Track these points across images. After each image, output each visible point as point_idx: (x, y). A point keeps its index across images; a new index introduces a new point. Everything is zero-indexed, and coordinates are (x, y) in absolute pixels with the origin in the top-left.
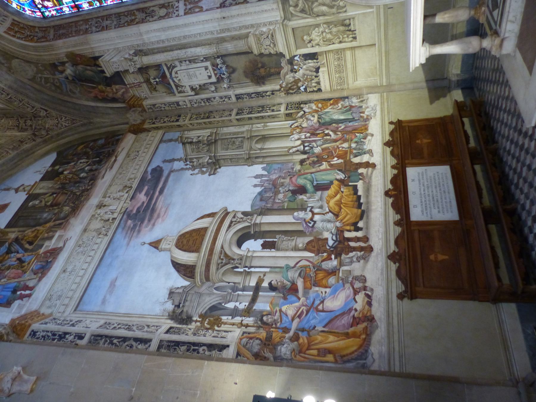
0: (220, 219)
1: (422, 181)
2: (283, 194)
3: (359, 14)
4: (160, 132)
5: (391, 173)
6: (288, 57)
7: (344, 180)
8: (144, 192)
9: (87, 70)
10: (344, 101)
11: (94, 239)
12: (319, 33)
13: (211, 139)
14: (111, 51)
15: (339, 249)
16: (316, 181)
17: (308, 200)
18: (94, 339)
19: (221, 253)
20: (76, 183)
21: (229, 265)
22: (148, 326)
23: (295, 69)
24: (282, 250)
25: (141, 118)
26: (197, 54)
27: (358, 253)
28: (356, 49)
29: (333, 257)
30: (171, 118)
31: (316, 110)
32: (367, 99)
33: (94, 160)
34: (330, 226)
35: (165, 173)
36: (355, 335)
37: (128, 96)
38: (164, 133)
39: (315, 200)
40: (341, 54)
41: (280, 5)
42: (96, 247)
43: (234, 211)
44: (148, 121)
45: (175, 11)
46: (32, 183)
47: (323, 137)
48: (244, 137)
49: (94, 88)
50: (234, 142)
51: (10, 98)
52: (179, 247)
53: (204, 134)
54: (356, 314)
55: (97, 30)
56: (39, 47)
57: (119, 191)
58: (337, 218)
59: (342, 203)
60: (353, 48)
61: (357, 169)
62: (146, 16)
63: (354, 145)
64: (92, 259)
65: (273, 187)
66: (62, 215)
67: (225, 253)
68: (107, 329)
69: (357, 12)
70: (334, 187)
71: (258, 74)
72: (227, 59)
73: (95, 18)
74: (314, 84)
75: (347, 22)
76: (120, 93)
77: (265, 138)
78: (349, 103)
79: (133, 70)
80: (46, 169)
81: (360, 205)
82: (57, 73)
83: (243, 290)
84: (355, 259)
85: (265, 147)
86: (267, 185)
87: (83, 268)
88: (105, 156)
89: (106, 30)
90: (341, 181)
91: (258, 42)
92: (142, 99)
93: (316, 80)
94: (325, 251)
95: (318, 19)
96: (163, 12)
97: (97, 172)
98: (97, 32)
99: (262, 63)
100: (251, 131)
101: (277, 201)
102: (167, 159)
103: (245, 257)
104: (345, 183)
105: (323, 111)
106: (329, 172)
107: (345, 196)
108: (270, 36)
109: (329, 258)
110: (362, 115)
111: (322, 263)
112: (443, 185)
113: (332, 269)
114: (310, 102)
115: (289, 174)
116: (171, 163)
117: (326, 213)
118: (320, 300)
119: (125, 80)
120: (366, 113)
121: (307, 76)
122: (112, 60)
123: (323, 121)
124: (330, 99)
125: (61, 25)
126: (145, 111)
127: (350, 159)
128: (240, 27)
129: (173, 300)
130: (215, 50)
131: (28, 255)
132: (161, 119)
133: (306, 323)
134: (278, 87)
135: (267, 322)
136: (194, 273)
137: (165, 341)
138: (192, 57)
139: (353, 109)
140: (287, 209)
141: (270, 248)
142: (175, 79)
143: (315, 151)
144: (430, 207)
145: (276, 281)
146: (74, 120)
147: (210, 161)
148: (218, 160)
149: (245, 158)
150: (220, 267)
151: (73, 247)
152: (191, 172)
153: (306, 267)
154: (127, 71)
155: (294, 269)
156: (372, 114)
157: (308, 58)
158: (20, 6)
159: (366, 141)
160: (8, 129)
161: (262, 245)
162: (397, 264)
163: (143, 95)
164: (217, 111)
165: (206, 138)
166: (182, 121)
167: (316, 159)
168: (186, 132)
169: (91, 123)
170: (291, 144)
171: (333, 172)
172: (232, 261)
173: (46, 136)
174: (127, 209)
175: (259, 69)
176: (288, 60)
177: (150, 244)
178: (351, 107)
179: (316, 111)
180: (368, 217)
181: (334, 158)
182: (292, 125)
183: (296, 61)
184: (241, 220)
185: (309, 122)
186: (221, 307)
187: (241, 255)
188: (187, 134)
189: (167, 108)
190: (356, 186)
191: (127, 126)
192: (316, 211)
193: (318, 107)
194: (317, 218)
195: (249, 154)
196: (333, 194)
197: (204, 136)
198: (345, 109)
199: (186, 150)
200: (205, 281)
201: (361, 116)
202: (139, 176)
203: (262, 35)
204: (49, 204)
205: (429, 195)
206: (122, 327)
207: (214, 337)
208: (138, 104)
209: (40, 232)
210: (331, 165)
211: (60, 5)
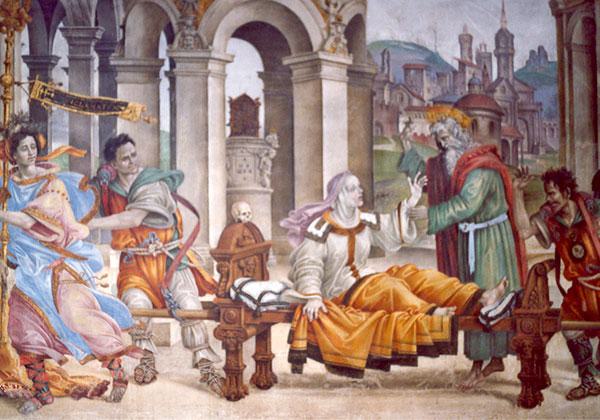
2: (427, 132)
7: (478, 313)
16: (476, 232)
27: (223, 364)
29: (210, 298)
34: (312, 285)
54: (52, 363)
58: (336, 301)
61: (520, 351)
83: (105, 69)
84: (202, 355)
86: (468, 76)
94: (225, 275)
106: (513, 270)
107: (416, 321)
111: (189, 270)
115: (510, 142)
117: (353, 269)
118: (85, 273)
127: (565, 329)
133: (21, 244)
135: (18, 148)
141: (233, 123)
145: (134, 155)
153: (178, 227)
161: (245, 98)
167: (568, 222)
181: (568, 277)
184: (333, 20)
186: (53, 23)
187: (211, 43)
190: (455, 352)
192: (364, 241)
196: (425, 285)
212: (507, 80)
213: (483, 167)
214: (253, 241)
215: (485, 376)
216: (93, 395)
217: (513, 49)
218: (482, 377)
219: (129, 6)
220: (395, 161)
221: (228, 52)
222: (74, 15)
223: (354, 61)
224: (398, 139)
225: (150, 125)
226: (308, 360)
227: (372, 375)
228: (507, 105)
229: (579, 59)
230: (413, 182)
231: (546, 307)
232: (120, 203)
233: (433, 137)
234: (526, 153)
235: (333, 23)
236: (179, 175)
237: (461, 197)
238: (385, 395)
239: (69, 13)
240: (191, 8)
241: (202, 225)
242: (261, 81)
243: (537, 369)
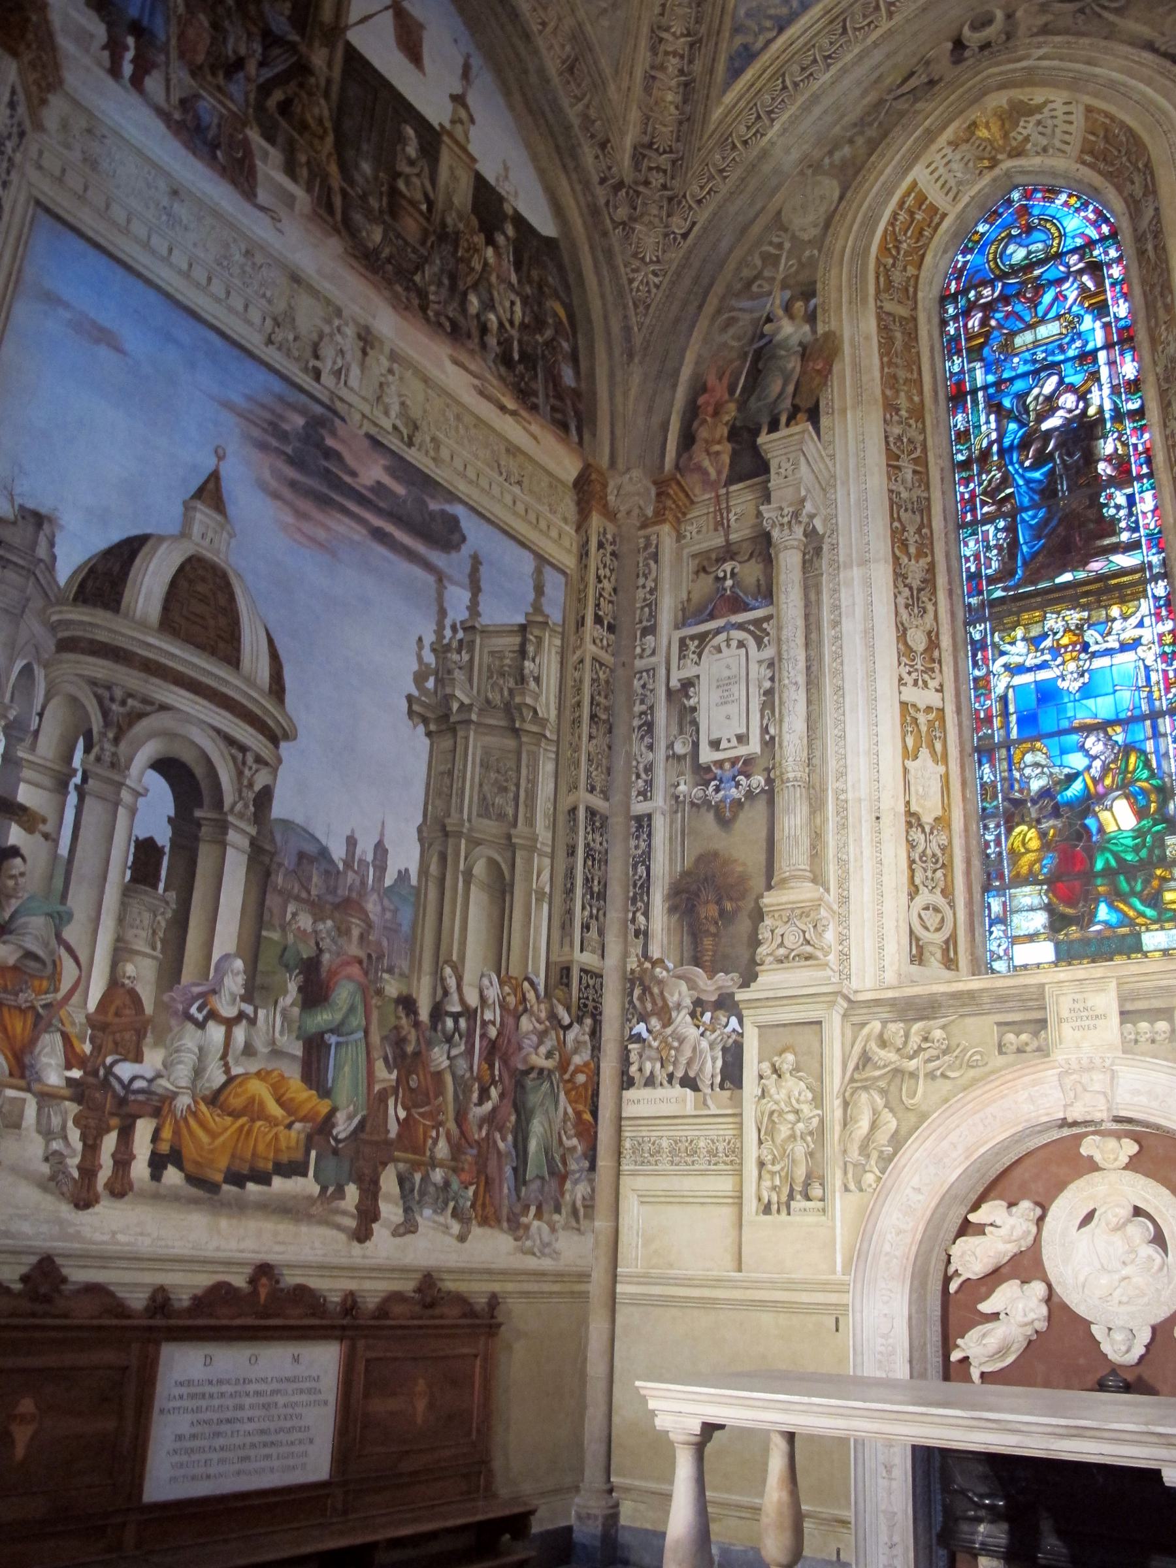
0: (259, 712)
1: (291, 1387)
2: (309, 930)
3: (833, 1228)
4: (569, 561)
5: (332, 1288)
6: (741, 995)
7: (330, 1133)
8: (387, 480)
9: (785, 385)
10: (585, 1155)
11: (263, 302)
12: (798, 1101)
13: (523, 720)
14: (830, 464)
15: (97, 1095)
16: (338, 1044)
17: (279, 1009)
19: (146, 701)
20: (453, 278)
21: (101, 722)
23: (702, 1015)
24: (124, 905)
25: (623, 509)
26: (786, 719)
27: (76, 1160)
28: (734, 1209)
29: (76, 1074)
30: (610, 602)
31: (568, 1064)
32: (578, 1230)
33: (516, 343)
34: (182, 1074)
35: (436, 557)
37: (692, 482)
38: (564, 573)
39: (277, 1035)
40: (725, 1163)
41: (890, 994)
42: (237, 303)
43: (280, 761)
44: (611, 529)
45: (914, 675)
46: (471, 148)
48: (515, 825)
49: (732, 390)
50: (505, 790)
51: (734, 147)
52: (188, 568)
53: (543, 698)
55: (891, 439)
56: (865, 264)
57: (403, 404)
58: (204, 1099)
59: (253, 1120)
60: (738, 1200)
61: (359, 1180)
62: (911, 589)
63: (438, 1175)
64: (198, 285)
65: (338, 900)
66: (358, 217)
67: (141, 715)
69: (838, 1224)
70: (310, 1097)
71: (703, 895)
72: (761, 805)
73: (925, 439)
74: (648, 1066)
75: (816, 1191)
76: (706, 463)
77: (503, 893)
78: (574, 1172)
79: (766, 515)
80: (511, 199)
81: (237, 1179)
82: (788, 294)
84: (56, 1145)
85: (473, 887)
86: (349, 881)
87: (175, 252)
88: (522, 378)
89: (888, 465)
90: (325, 1125)
91: (798, 912)
92: (678, 521)
93: (661, 1075)
94: (97, 1048)
95: (838, 1102)
96: (918, 640)
97: (477, 348)
98: (886, 437)
99: (736, 912)
100: (532, 849)
101: (291, 908)
102: (483, 570)
103: (117, 778)
106: (363, 1088)
107: (276, 1136)
108: (808, 949)
109: (73, 1061)
110: (533, 1209)
112: (268, 1457)
113: (32, 1066)
114: (596, 1049)
115: (374, 956)
116: (467, 581)
117: (226, 1065)
119: (741, 485)
120: (536, 1223)
121: (677, 1049)
122: (802, 459)
123: (529, 1083)
124: (595, 1113)
125: (916, 339)
126: (644, 526)
128: (847, 862)
129: (14, 523)
130: (791, 775)
131: (247, 94)
132: (612, 571)
134: (655, 952)
136: (95, 605)
138: (781, 703)
139: (554, 1184)
140: (258, 940)
141: (135, 867)
142: (723, 636)
143: (436, 1049)
144: (198, 1410)
145: (22, 874)
146: (648, 307)
147: (455, 706)
148: (453, 731)
149: (448, 821)
150: (100, 691)
151: (249, 233)
152: (429, 638)
154: (767, 498)
155: (54, 942)
156: (529, 1243)
157: (729, 1059)
158: (978, 242)
159: (446, 1218)
160: (648, 118)
162: (18, 1287)
163: (690, 529)
164: (610, 748)
165: (529, 701)
167: (410, 1049)
168: (558, 642)
169: (631, 356)
170: (469, 976)
171: (362, 1099)
172: (111, 735)
173: (612, 219)
174: (343, 419)
175: (719, 902)
176: (732, 995)
177: (215, 476)
178: (563, 1178)
179: (563, 1066)
180: (194, 1202)
181: (405, 1108)
182: (532, 984)
183: (724, 1020)
184: (245, 782)
185: (535, 1038)
187: (128, 767)
188: (551, 645)
189: (640, 594)
190: (305, 1175)
191: (604, 462)
192: (240, 1034)
193: (578, 1070)
194: (216, 1032)
195: (459, 835)
196: (288, 1095)
197: (537, 696)
198: (557, 1158)
199: (500, 631)
200: (60, 635)
201: (527, 1208)
202: (440, 474)
203: (815, 927)
204: (401, 185)
205: (241, 1407)
208: (665, 508)
209: (316, 142)
210: (382, 1097)
211: (969, 350)
223: (258, 833)
224: (283, 928)
241: (83, 983)
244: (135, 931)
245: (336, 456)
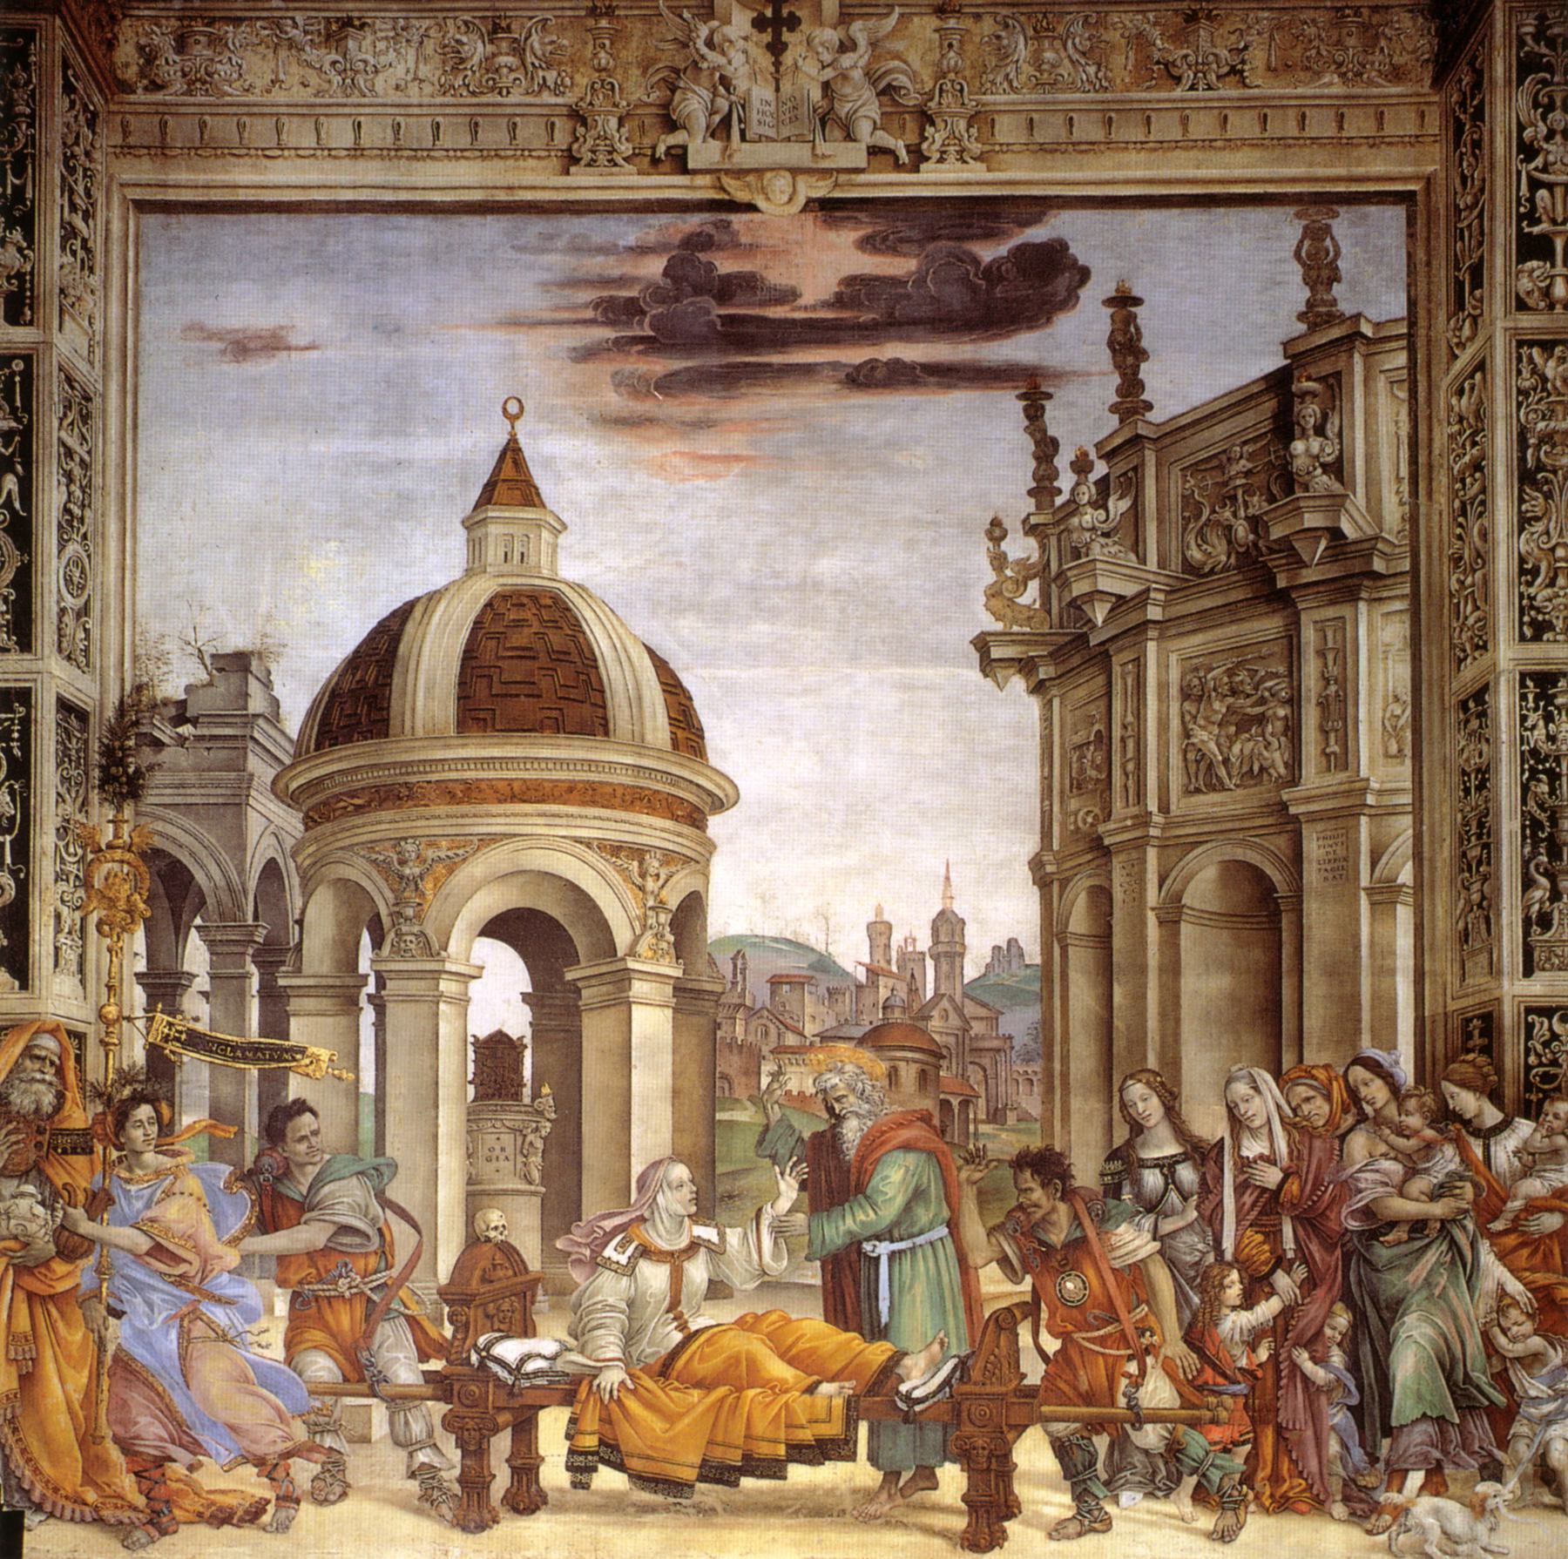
2: (810, 1090)
11: (547, 97)
16: (892, 1256)
18: (13, 374)
22: (85, 611)
27: (457, 1472)
29: (436, 1365)
35: (1018, 348)
36: (94, 1467)
39: (767, 1258)
47: (1240, 1262)
48: (1294, 780)
54: (178, 1469)
58: (646, 1369)
59: (740, 1389)
61: (965, 1457)
63: (1151, 1437)
68: (61, 420)
77: (1275, 916)
81: (720, 1473)
83: (273, 997)
84: (422, 1457)
85: (1185, 929)
86: (883, 993)
94: (463, 1327)
104: (865, 1403)
105: (1484, 1246)
109: (428, 1350)
110: (1416, 1479)
111: (402, 1319)
115: (955, 1102)
120: (1427, 1502)
127: (1046, 1420)
135: (128, 1125)
136: (349, 739)
137: (28, 713)
141: (479, 1080)
145: (315, 1133)
147: (1100, 613)
148: (1102, 658)
149: (1101, 829)
153: (385, 1252)
159: (1181, 1504)
166: (1525, 284)
167: (1057, 1237)
177: (511, 453)
181: (1055, 1335)
186: (184, 917)
190: (852, 1457)
192: (697, 1272)
196: (801, 1346)
201: (1397, 1475)
206: (73, 488)
207: (58, 916)
212: (951, 999)
213: (907, 1147)
214: (510, 1272)
215: (903, 1496)
216: (241, 1520)
217: (963, 944)
218: (899, 1500)
219: (311, 886)
220: (752, 1138)
221: (472, 962)
222: (219, 903)
224: (758, 1100)
225: (343, 1085)
226: (601, 1467)
227: (708, 1492)
228: (951, 1040)
229: (1080, 960)
230: (782, 1174)
231: (1015, 1383)
232: (292, 1212)
233: (820, 1096)
234: (983, 1122)
235: (652, 908)
236: (388, 1165)
237: (867, 1198)
238: (731, 1527)
239: (210, 901)
240: (413, 886)
242: (527, 1009)
243: (997, 1485)
244: (494, 1165)
245: (749, 283)
